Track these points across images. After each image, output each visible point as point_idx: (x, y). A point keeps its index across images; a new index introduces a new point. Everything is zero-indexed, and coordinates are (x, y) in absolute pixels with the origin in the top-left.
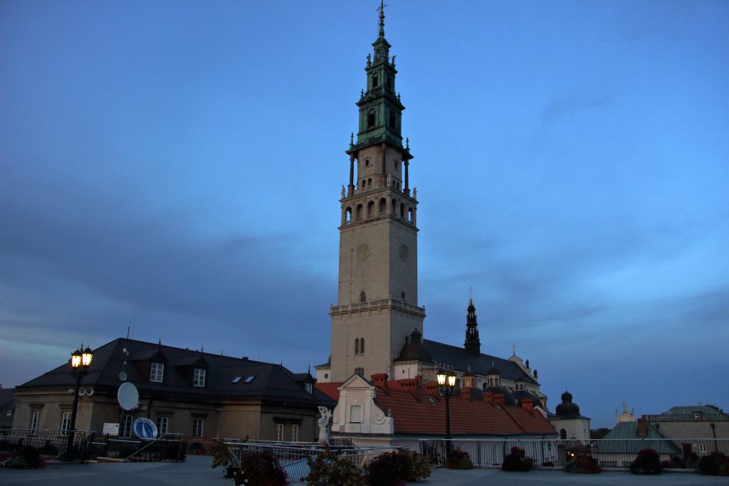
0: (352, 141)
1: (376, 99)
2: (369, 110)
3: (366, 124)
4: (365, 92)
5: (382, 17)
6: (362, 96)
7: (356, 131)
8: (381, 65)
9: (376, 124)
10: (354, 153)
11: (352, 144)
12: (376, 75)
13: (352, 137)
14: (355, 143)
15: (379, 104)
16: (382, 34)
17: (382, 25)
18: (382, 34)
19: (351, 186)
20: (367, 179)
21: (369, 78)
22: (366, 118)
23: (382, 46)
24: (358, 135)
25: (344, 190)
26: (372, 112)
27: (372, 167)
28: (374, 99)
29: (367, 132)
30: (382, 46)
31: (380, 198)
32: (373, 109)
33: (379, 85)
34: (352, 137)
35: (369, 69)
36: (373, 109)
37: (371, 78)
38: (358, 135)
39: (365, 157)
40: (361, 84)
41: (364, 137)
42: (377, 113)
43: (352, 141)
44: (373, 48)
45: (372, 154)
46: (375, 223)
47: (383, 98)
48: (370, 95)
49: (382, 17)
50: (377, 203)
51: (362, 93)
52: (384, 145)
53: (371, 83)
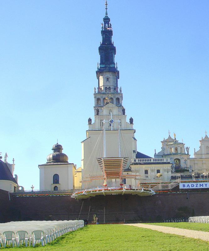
0: (98, 67)
5: (106, 4)
7: (99, 62)
10: (100, 72)
11: (98, 68)
16: (107, 14)
17: (106, 9)
18: (107, 14)
19: (99, 88)
23: (107, 20)
25: (95, 89)
30: (107, 20)
39: (106, 76)
40: (99, 40)
41: (104, 66)
43: (98, 67)
45: (109, 75)
49: (106, 4)
50: (115, 99)
51: (101, 43)
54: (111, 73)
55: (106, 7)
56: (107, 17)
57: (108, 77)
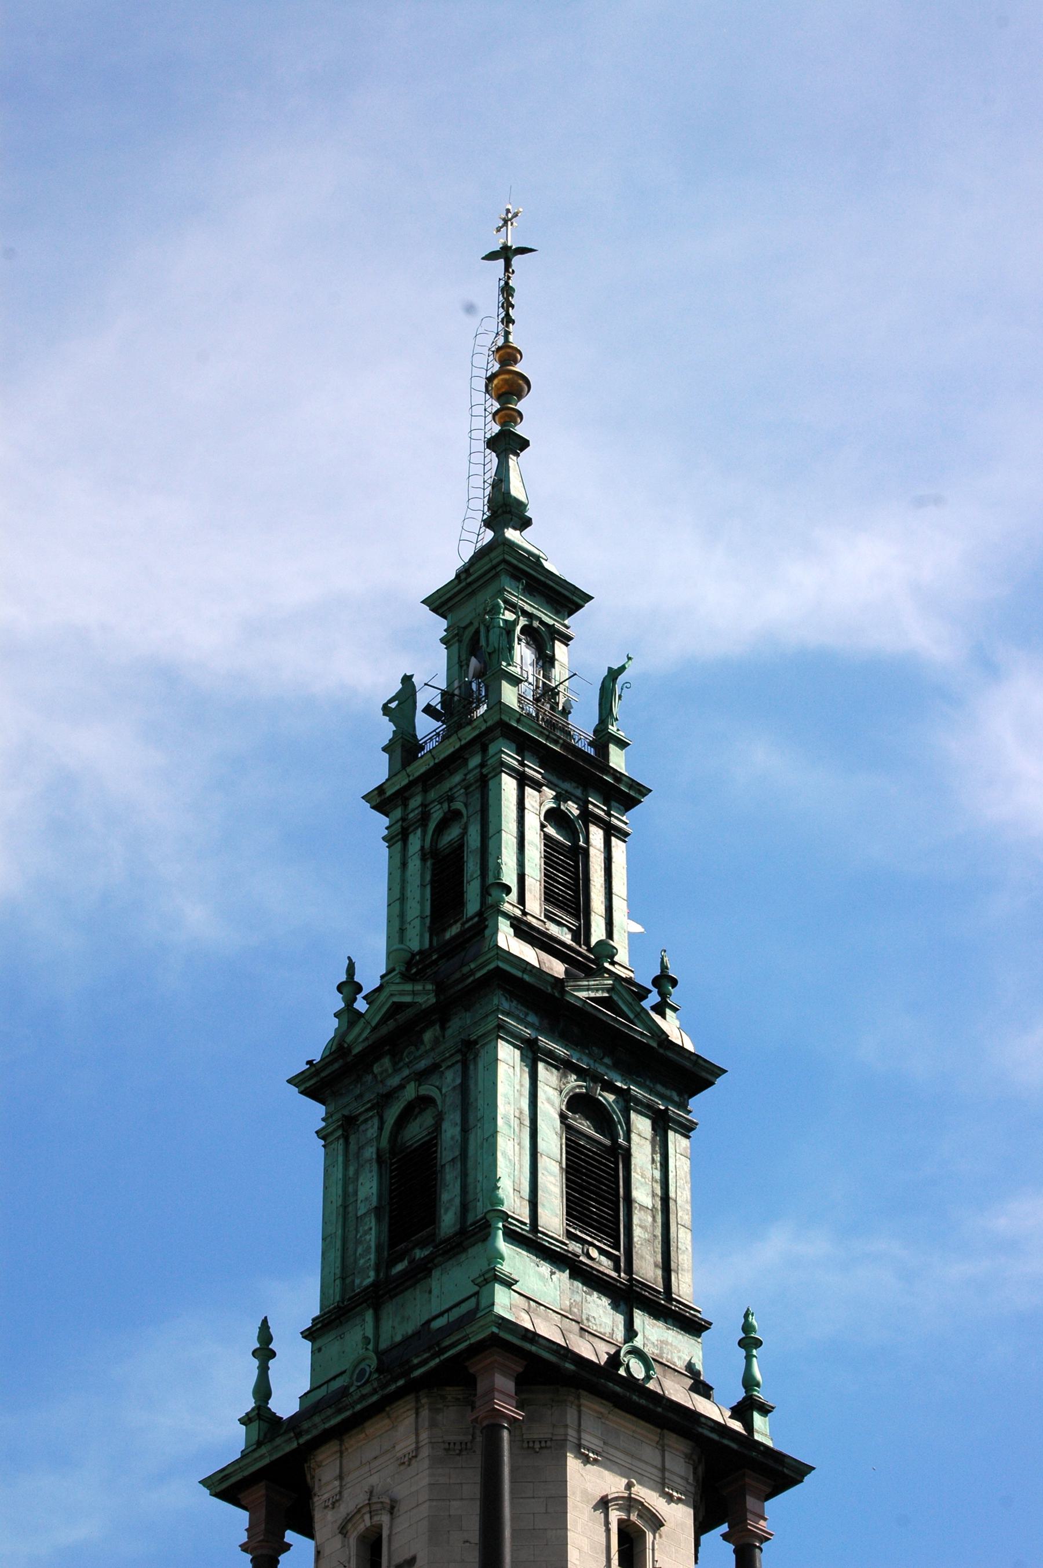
0: (263, 1391)
3: (371, 1234)
6: (348, 1015)
12: (453, 833)
13: (265, 1353)
21: (399, 867)
22: (369, 1187)
24: (309, 1334)
34: (265, 1353)
37: (415, 864)
38: (309, 1334)
42: (451, 1131)
43: (263, 1391)
48: (405, 993)
51: (350, 987)
53: (418, 905)
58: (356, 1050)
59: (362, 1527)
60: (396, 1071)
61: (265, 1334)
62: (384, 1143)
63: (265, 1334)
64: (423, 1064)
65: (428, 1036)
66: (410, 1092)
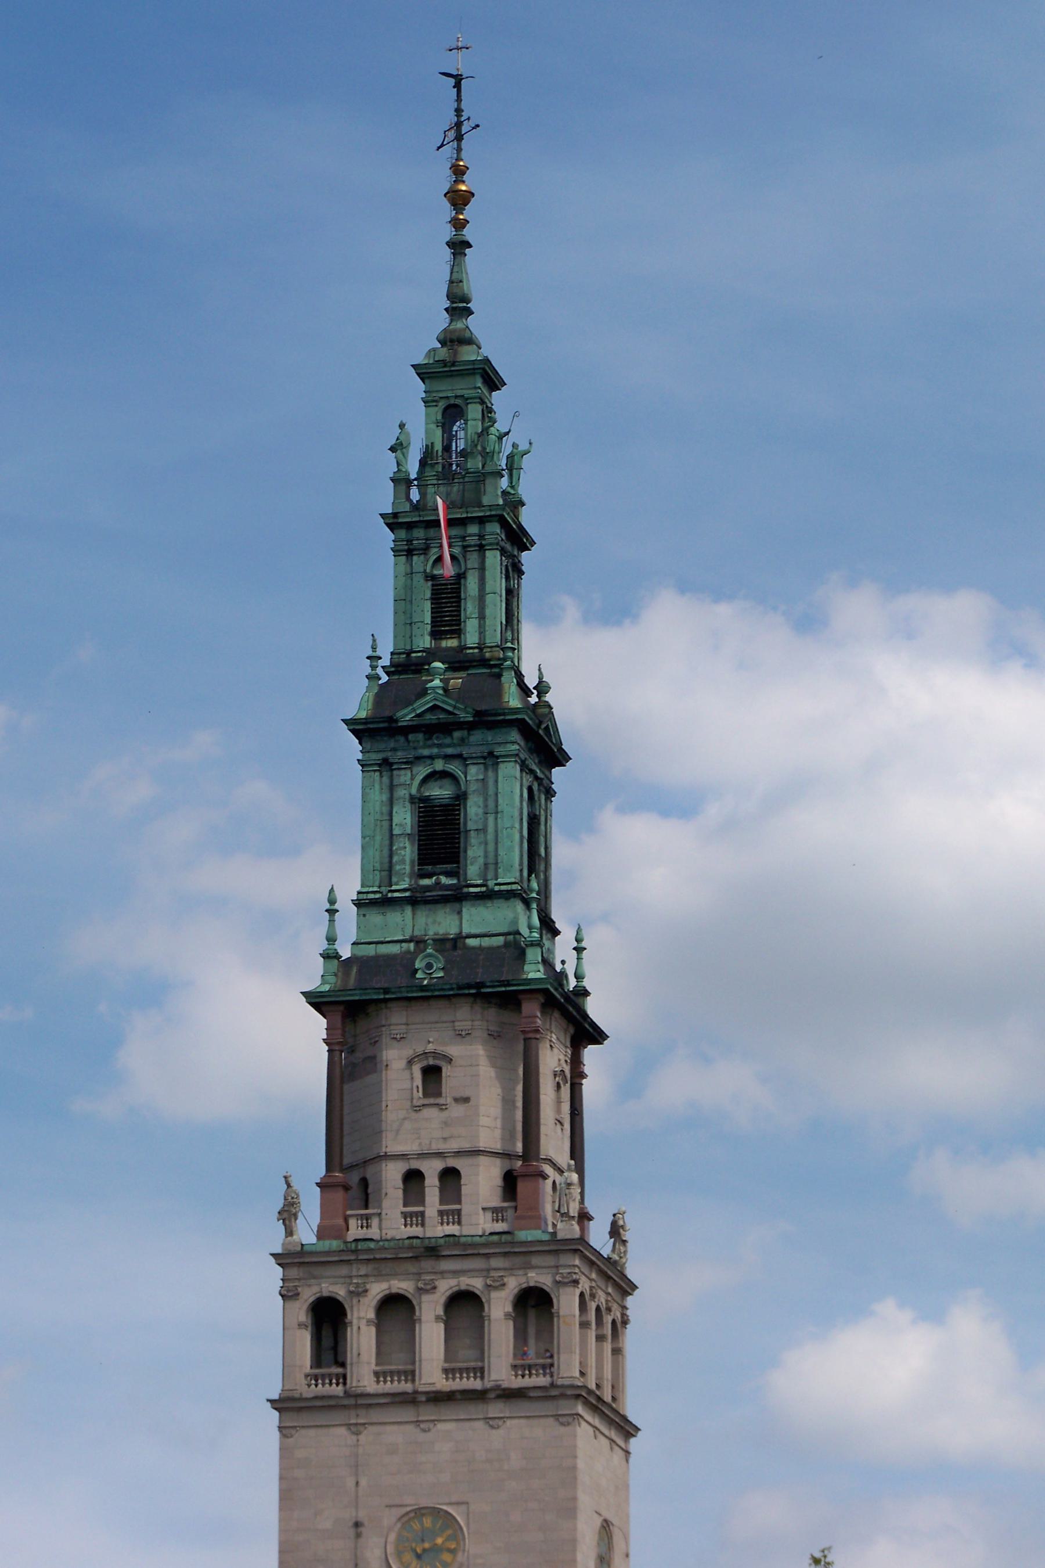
0: (331, 939)
1: (471, 727)
2: (422, 771)
3: (407, 852)
4: (386, 661)
8: (481, 521)
9: (473, 871)
11: (329, 956)
13: (332, 912)
14: (346, 953)
15: (491, 759)
17: (459, 247)
20: (431, 1170)
22: (405, 818)
26: (440, 792)
27: (457, 1111)
28: (460, 725)
29: (416, 900)
31: (514, 1284)
32: (444, 775)
33: (471, 638)
35: (410, 526)
36: (444, 775)
38: (359, 904)
43: (331, 939)
44: (419, 387)
46: (495, 1409)
47: (515, 735)
49: (459, 200)
51: (373, 658)
52: (531, 1008)
54: (465, 1015)
55: (459, 225)
56: (467, 340)
57: (435, 1054)
58: (400, 724)
59: (425, 1063)
60: (425, 747)
61: (332, 901)
62: (414, 791)
63: (332, 901)
64: (450, 751)
65: (457, 734)
66: (439, 765)
